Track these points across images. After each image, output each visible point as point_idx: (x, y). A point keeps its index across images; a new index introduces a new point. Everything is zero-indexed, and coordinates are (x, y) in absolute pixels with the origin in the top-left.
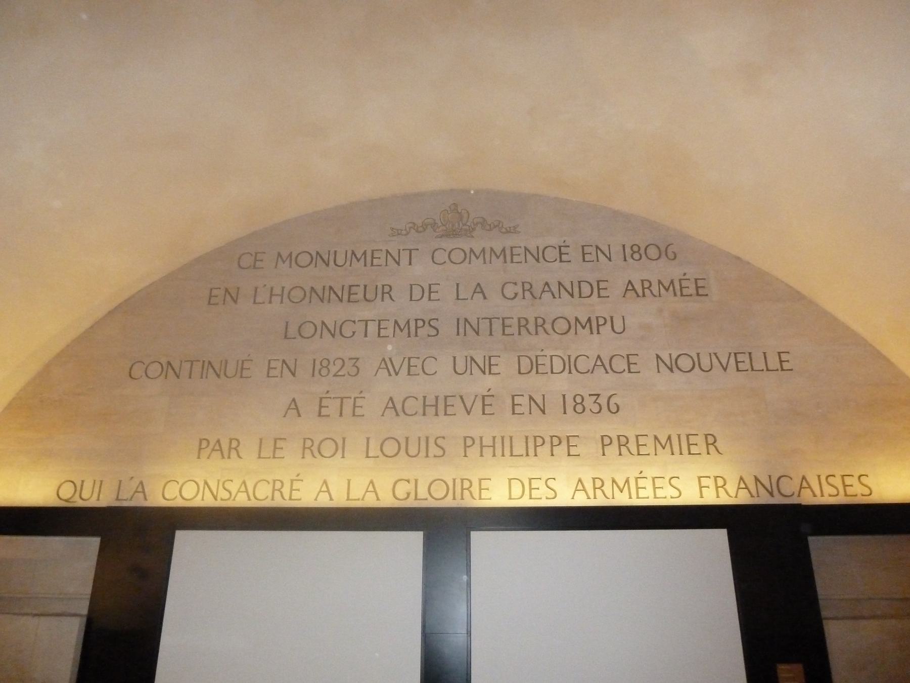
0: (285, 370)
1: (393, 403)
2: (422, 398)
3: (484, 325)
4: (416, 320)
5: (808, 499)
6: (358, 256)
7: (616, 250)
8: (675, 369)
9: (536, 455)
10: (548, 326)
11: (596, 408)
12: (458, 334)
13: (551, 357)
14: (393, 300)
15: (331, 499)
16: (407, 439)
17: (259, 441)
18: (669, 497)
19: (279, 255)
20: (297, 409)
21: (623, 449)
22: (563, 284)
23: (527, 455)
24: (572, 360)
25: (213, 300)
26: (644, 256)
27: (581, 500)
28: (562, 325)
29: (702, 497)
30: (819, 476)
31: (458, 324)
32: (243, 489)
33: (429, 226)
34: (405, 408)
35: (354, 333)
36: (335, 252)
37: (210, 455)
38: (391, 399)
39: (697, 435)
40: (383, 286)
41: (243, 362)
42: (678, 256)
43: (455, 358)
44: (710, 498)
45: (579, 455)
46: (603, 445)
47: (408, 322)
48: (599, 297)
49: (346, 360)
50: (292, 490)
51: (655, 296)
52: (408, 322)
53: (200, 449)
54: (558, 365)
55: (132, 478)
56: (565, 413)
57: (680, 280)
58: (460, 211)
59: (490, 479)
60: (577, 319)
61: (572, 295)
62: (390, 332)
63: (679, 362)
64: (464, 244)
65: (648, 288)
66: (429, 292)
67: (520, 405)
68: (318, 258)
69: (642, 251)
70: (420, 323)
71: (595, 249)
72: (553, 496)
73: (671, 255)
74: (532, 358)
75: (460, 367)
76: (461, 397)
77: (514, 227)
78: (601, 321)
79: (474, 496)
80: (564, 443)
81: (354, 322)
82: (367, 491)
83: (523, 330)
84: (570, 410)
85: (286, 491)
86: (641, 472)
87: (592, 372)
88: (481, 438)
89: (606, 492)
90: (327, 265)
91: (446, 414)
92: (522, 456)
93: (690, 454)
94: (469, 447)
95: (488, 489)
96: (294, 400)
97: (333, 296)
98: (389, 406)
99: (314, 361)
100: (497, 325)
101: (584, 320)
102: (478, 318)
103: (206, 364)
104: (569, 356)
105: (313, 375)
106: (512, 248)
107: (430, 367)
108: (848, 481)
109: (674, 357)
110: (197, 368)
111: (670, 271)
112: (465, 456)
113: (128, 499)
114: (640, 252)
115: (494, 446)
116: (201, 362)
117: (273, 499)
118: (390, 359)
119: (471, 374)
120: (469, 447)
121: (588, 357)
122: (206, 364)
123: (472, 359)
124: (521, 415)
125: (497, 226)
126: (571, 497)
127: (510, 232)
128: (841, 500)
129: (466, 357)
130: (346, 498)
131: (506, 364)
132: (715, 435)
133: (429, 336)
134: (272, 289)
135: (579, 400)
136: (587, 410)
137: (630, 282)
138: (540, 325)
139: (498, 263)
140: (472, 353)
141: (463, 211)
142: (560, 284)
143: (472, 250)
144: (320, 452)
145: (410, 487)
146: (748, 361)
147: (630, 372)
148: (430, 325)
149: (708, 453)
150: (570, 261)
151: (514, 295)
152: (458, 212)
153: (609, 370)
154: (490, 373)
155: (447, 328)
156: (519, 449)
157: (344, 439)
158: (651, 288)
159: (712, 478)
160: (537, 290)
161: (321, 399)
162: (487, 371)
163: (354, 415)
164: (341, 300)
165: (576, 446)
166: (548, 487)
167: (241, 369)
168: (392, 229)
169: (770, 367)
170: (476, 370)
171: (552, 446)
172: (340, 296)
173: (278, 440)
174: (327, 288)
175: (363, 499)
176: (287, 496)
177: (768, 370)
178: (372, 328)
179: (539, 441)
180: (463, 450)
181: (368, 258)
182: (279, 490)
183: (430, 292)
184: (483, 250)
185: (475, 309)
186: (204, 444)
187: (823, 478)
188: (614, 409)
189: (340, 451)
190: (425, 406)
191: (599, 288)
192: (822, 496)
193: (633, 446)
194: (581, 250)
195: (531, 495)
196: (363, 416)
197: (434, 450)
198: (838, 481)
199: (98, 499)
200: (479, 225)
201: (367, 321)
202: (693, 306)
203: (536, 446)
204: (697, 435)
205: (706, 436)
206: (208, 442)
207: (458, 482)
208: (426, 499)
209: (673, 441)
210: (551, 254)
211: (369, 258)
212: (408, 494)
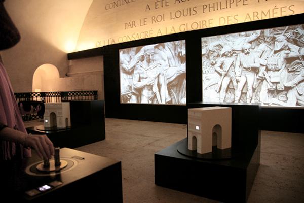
85: (149, 34)
115: (214, 7)
203: (230, 4)
207: (201, 22)
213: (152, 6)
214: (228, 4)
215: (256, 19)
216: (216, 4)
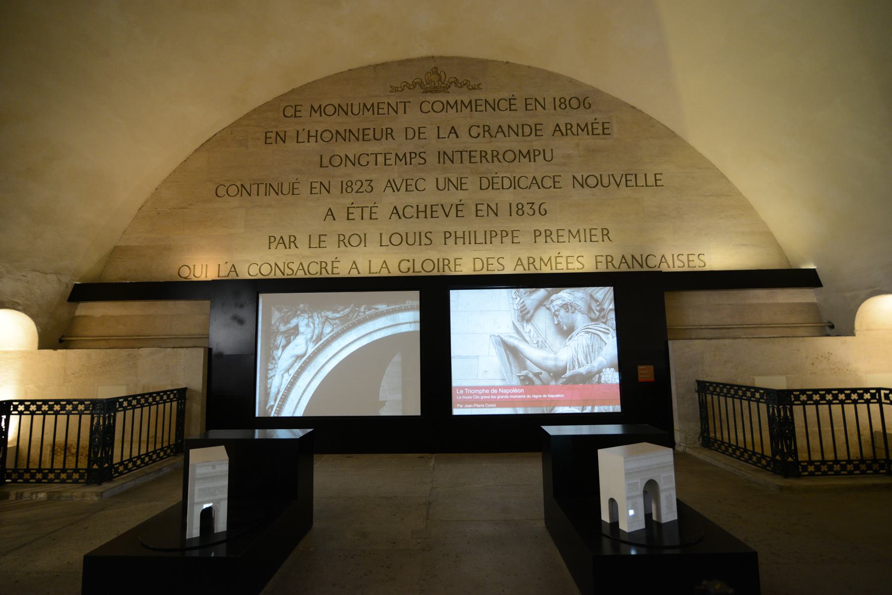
0: (323, 189)
1: (396, 210)
3: (457, 156)
4: (410, 153)
5: (664, 268)
6: (369, 108)
7: (549, 101)
8: (585, 185)
9: (491, 243)
10: (500, 157)
11: (531, 212)
12: (439, 163)
13: (502, 177)
14: (394, 139)
16: (407, 233)
17: (309, 237)
19: (312, 107)
20: (332, 215)
21: (548, 239)
23: (486, 243)
26: (568, 106)
27: (520, 270)
30: (673, 255)
32: (301, 268)
33: (418, 85)
34: (405, 213)
35: (368, 162)
36: (352, 104)
37: (277, 246)
38: (395, 207)
39: (597, 229)
40: (387, 129)
41: (293, 183)
42: (592, 105)
43: (437, 179)
45: (519, 243)
46: (535, 237)
47: (405, 155)
48: (536, 135)
50: (333, 268)
51: (574, 135)
52: (405, 155)
53: (270, 243)
54: (507, 183)
55: (227, 263)
56: (511, 215)
60: (520, 151)
61: (517, 135)
62: (392, 162)
63: (588, 181)
65: (570, 129)
66: (419, 133)
67: (481, 210)
68: (339, 109)
69: (567, 103)
70: (413, 155)
72: (502, 269)
73: (587, 106)
75: (441, 186)
76: (442, 205)
78: (537, 153)
79: (451, 269)
80: (510, 234)
81: (368, 155)
83: (484, 160)
84: (514, 213)
85: (329, 268)
86: (559, 253)
87: (529, 188)
88: (456, 232)
89: (536, 266)
90: (347, 114)
91: (432, 217)
93: (591, 241)
94: (447, 238)
96: (330, 209)
99: (342, 182)
100: (466, 156)
102: (453, 152)
103: (268, 186)
104: (514, 177)
105: (342, 192)
106: (476, 100)
108: (691, 258)
109: (585, 177)
110: (262, 188)
111: (584, 117)
112: (445, 244)
115: (464, 238)
117: (321, 274)
118: (394, 180)
119: (449, 190)
120: (447, 238)
121: (527, 178)
122: (268, 186)
123: (449, 179)
127: (474, 88)
129: (445, 178)
131: (471, 183)
132: (608, 229)
134: (309, 131)
135: (520, 206)
136: (525, 213)
137: (557, 125)
138: (495, 155)
139: (466, 111)
140: (449, 175)
141: (442, 73)
142: (509, 126)
143: (448, 102)
144: (349, 243)
145: (410, 264)
146: (634, 180)
147: (554, 188)
148: (420, 157)
150: (516, 110)
152: (438, 74)
154: (461, 189)
155: (432, 159)
157: (365, 235)
158: (572, 129)
159: (605, 257)
160: (493, 131)
161: (348, 208)
165: (518, 237)
166: (499, 263)
167: (293, 190)
171: (502, 237)
172: (357, 136)
173: (321, 236)
174: (347, 131)
175: (379, 273)
176: (330, 272)
177: (646, 186)
178: (381, 159)
179: (494, 234)
180: (444, 240)
181: (374, 109)
182: (324, 268)
183: (419, 133)
184: (456, 102)
185: (450, 144)
186: (272, 239)
188: (543, 212)
189: (363, 243)
190: (418, 212)
191: (536, 130)
192: (674, 267)
193: (554, 237)
196: (377, 219)
197: (425, 241)
198: (684, 258)
200: (454, 84)
201: (376, 154)
202: (600, 142)
203: (491, 237)
207: (441, 260)
208: (421, 272)
210: (504, 105)
213: (341, 214)
214: (488, 237)
215: (532, 271)
216: (467, 234)
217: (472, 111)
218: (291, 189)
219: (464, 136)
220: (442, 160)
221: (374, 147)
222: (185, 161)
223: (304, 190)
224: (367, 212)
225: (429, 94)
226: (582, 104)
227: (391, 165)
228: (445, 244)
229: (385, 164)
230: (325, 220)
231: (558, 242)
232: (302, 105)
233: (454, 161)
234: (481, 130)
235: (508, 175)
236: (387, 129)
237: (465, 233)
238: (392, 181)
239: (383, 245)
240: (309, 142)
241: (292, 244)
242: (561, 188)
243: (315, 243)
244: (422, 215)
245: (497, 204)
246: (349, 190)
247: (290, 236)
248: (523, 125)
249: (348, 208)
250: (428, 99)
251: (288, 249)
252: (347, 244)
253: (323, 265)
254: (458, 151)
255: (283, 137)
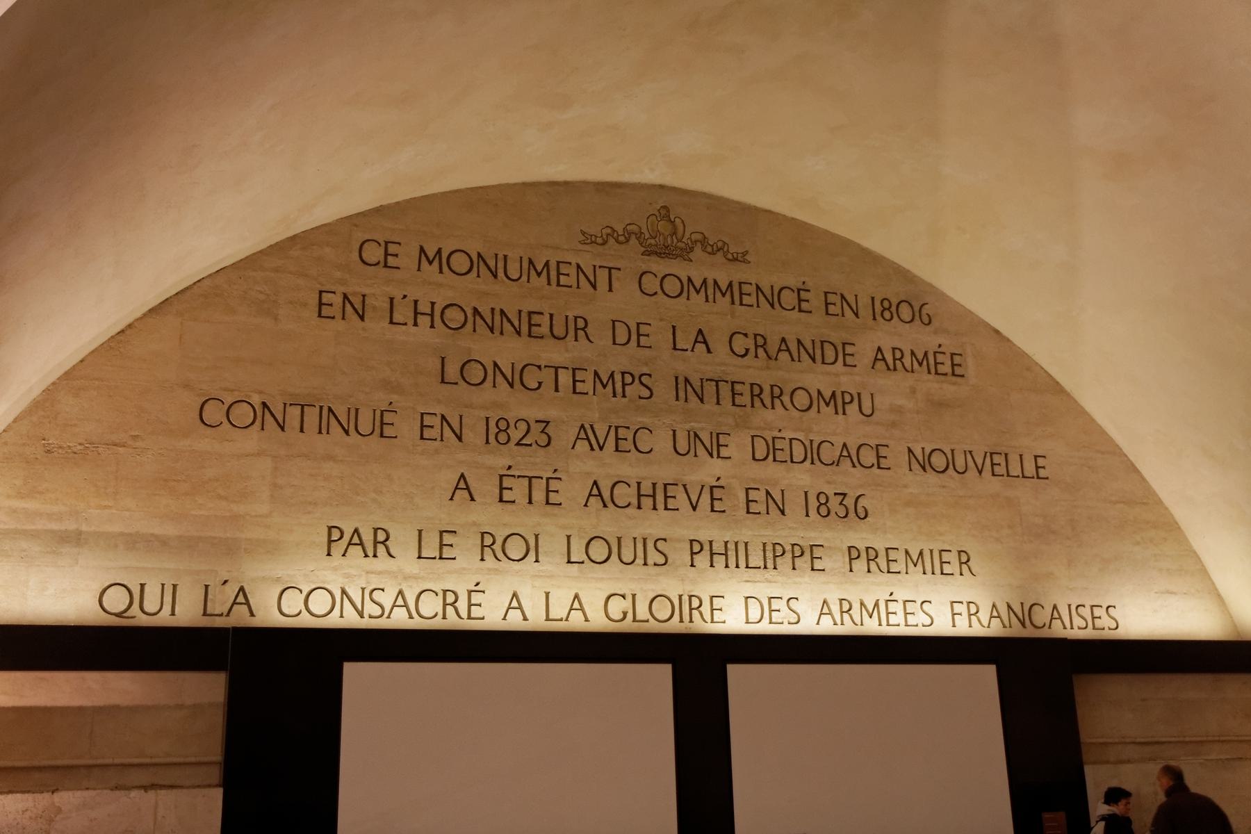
2: (636, 485)
3: (710, 388)
4: (623, 373)
5: (1058, 631)
6: (539, 269)
7: (864, 301)
9: (775, 568)
12: (677, 399)
14: (590, 341)
15: (525, 619)
16: (619, 539)
18: (920, 625)
19: (422, 250)
20: (468, 488)
21: (873, 564)
22: (803, 342)
23: (765, 567)
24: (815, 446)
25: (326, 311)
27: (827, 627)
28: (801, 399)
29: (954, 626)
30: (1069, 606)
31: (677, 384)
33: (633, 237)
34: (614, 497)
35: (540, 383)
36: (505, 257)
38: (595, 483)
39: (950, 551)
40: (576, 318)
41: (382, 412)
42: (933, 320)
43: (674, 431)
44: (963, 628)
45: (824, 570)
46: (851, 559)
49: (533, 424)
50: (470, 605)
51: (908, 371)
52: (612, 375)
53: (330, 541)
55: (226, 582)
56: (807, 515)
57: (935, 353)
58: (673, 220)
59: (723, 597)
60: (819, 392)
64: (681, 269)
66: (638, 334)
67: (756, 501)
69: (893, 309)
70: (628, 379)
71: (840, 298)
74: (768, 439)
75: (682, 445)
76: (684, 486)
77: (742, 253)
78: (848, 399)
81: (539, 367)
82: (571, 609)
83: (757, 403)
84: (813, 512)
85: (462, 605)
86: (891, 594)
87: (837, 465)
88: (711, 542)
90: (495, 276)
92: (760, 568)
93: (942, 573)
94: (696, 553)
95: (721, 610)
96: (462, 476)
97: (507, 326)
98: (593, 493)
100: (725, 390)
101: (827, 395)
102: (702, 379)
103: (325, 412)
104: (811, 441)
106: (740, 283)
107: (644, 441)
108: (1097, 612)
109: (927, 451)
110: (312, 416)
113: (222, 613)
114: (891, 310)
115: (726, 555)
116: (318, 408)
117: (444, 617)
118: (592, 426)
119: (696, 456)
121: (833, 445)
122: (325, 412)
123: (696, 435)
124: (757, 515)
125: (721, 249)
126: (816, 622)
127: (736, 260)
128: (1089, 634)
130: (545, 618)
131: (737, 446)
133: (640, 398)
134: (416, 302)
136: (833, 513)
137: (879, 349)
141: (677, 219)
143: (690, 280)
146: (1004, 464)
148: (641, 383)
149: (961, 574)
150: (811, 312)
151: (745, 350)
152: (670, 220)
153: (857, 464)
154: (719, 457)
155: (663, 390)
156: (756, 560)
157: (537, 536)
158: (903, 360)
159: (965, 604)
160: (773, 347)
161: (501, 476)
162: (715, 454)
163: (547, 503)
164: (519, 333)
167: (381, 428)
168: (583, 233)
169: (1027, 474)
170: (701, 451)
171: (794, 557)
175: (567, 620)
178: (565, 378)
181: (551, 272)
183: (639, 335)
184: (705, 281)
185: (696, 364)
186: (335, 535)
187: (1073, 608)
188: (862, 514)
190: (639, 496)
191: (843, 352)
192: (1072, 628)
193: (882, 561)
194: (823, 298)
195: (771, 619)
196: (560, 504)
198: (1086, 612)
199: (173, 614)
200: (699, 244)
201: (556, 369)
202: (948, 389)
203: (775, 557)
204: (950, 551)
205: (960, 552)
206: (342, 533)
207: (685, 598)
208: (647, 621)
209: (924, 557)
210: (789, 298)
211: (553, 273)
212: (625, 614)
213: (485, 488)
214: (770, 555)
216: (731, 546)
217: (733, 303)
218: (378, 423)
219: (721, 349)
220: (682, 394)
221: (552, 353)
222: (122, 331)
223: (406, 428)
224: (539, 487)
225: (654, 258)
226: (917, 314)
227: (587, 394)
228: (692, 565)
229: (574, 392)
230: (451, 499)
231: (889, 572)
232: (399, 244)
233: (705, 399)
234: (750, 343)
235: (801, 436)
236: (576, 318)
237: (729, 545)
238: (587, 426)
239: (572, 560)
240: (416, 324)
241: (381, 549)
242: (889, 469)
243: (431, 549)
244: (646, 502)
245: (782, 491)
246: (503, 438)
247: (376, 530)
248: (822, 342)
249: (501, 476)
250: (654, 268)
251: (371, 559)
252: (500, 555)
253: (449, 599)
254: (711, 380)
255: (359, 306)
